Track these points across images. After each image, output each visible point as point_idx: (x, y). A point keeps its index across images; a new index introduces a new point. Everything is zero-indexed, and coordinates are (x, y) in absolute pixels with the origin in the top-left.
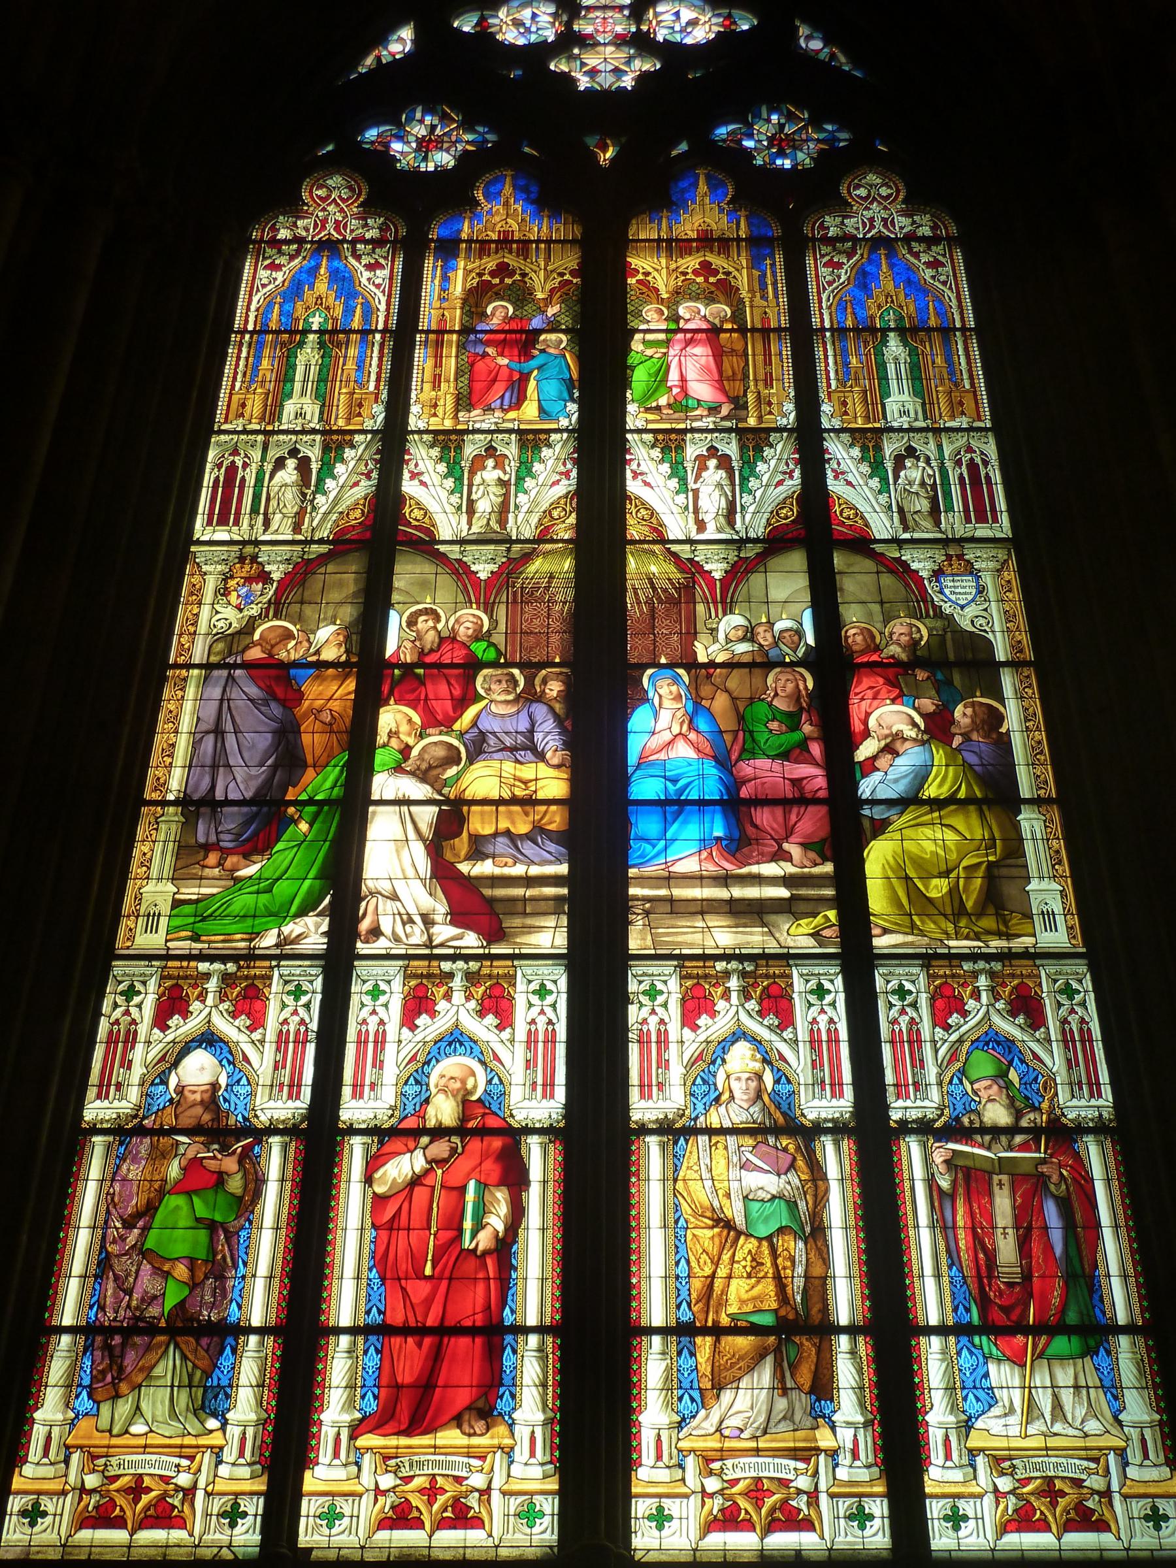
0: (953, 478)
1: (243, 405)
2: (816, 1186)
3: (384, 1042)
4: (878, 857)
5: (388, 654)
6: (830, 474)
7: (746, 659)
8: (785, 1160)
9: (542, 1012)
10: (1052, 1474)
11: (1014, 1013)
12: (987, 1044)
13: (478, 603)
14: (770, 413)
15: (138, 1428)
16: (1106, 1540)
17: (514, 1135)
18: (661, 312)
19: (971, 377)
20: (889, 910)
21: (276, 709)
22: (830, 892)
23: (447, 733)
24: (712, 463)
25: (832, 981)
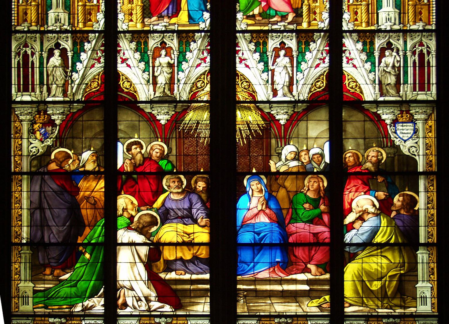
1: (26, 14)
4: (351, 271)
5: (119, 166)
6: (345, 60)
7: (295, 170)
14: (315, 20)
20: (353, 296)
21: (67, 197)
22: (327, 287)
23: (150, 210)
24: (282, 53)
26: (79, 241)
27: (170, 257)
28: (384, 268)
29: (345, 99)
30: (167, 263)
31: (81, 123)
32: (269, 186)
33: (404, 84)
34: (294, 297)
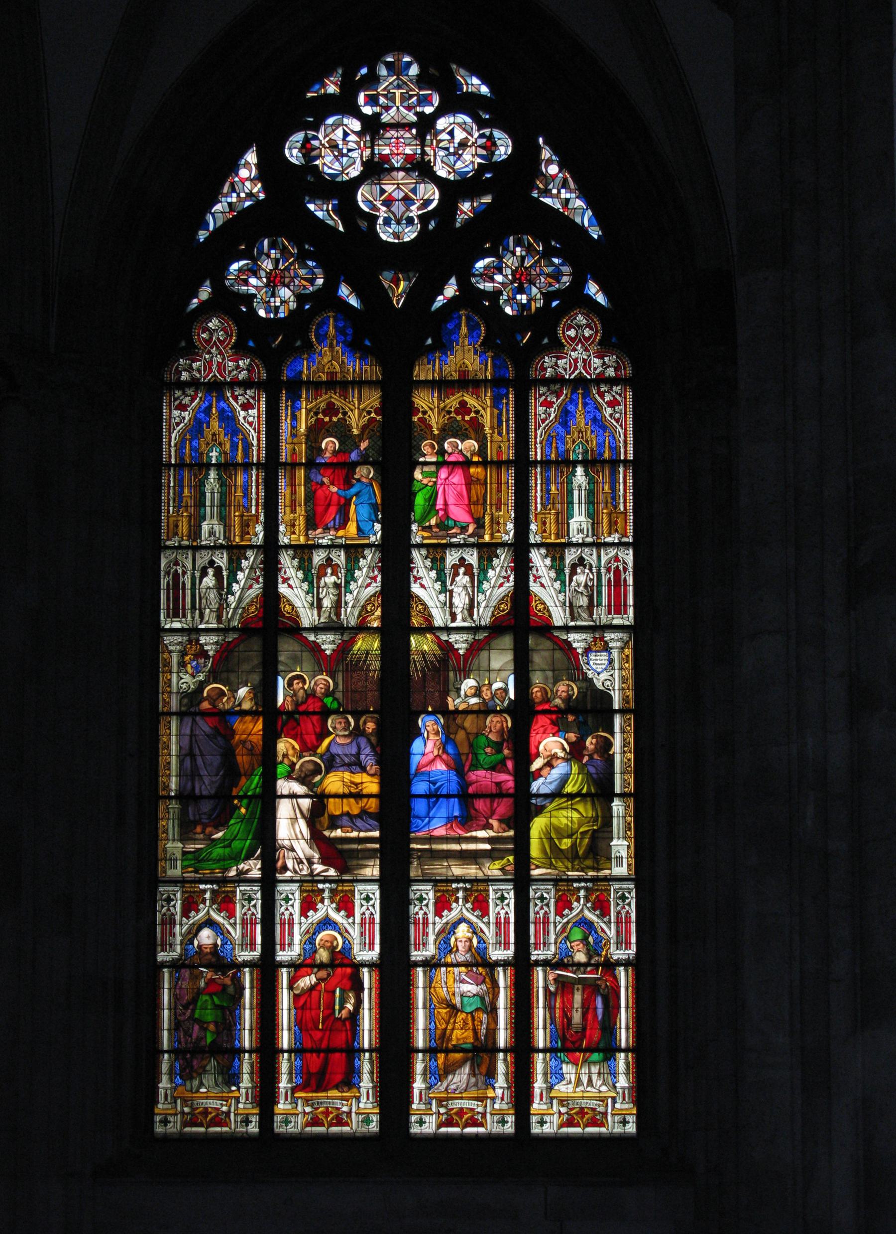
0: (604, 581)
1: (177, 526)
2: (494, 991)
3: (293, 923)
4: (538, 825)
6: (532, 578)
7: (476, 708)
8: (480, 978)
9: (368, 909)
13: (326, 672)
14: (499, 531)
15: (203, 1090)
16: (603, 1130)
18: (433, 447)
19: (625, 502)
22: (511, 846)
23: (314, 756)
24: (462, 570)
26: (234, 794)
29: (532, 624)
31: (236, 654)
32: (446, 728)
33: (597, 606)
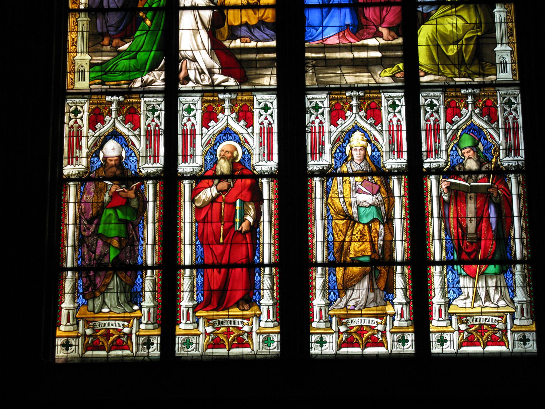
2: (389, 200)
3: (195, 134)
4: (425, 32)
8: (376, 188)
9: (266, 118)
10: (483, 323)
11: (481, 115)
12: (469, 130)
15: (105, 310)
17: (257, 177)
20: (428, 62)
22: (400, 54)
25: (400, 100)
26: (140, 6)
27: (235, 22)
28: (460, 29)
30: (231, 30)
34: (366, 66)
